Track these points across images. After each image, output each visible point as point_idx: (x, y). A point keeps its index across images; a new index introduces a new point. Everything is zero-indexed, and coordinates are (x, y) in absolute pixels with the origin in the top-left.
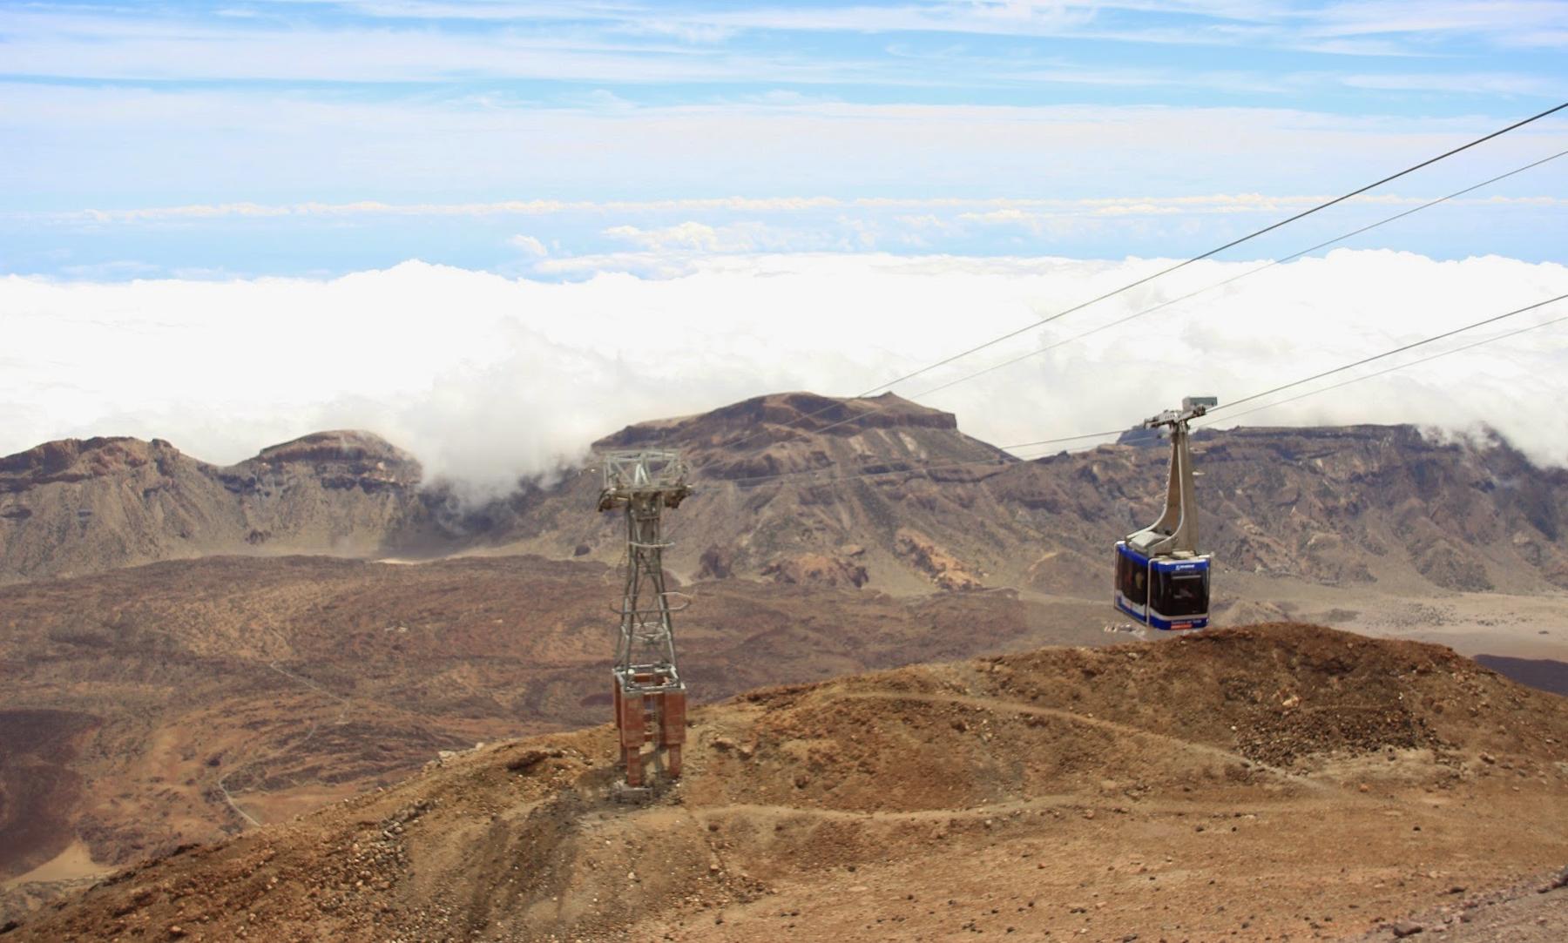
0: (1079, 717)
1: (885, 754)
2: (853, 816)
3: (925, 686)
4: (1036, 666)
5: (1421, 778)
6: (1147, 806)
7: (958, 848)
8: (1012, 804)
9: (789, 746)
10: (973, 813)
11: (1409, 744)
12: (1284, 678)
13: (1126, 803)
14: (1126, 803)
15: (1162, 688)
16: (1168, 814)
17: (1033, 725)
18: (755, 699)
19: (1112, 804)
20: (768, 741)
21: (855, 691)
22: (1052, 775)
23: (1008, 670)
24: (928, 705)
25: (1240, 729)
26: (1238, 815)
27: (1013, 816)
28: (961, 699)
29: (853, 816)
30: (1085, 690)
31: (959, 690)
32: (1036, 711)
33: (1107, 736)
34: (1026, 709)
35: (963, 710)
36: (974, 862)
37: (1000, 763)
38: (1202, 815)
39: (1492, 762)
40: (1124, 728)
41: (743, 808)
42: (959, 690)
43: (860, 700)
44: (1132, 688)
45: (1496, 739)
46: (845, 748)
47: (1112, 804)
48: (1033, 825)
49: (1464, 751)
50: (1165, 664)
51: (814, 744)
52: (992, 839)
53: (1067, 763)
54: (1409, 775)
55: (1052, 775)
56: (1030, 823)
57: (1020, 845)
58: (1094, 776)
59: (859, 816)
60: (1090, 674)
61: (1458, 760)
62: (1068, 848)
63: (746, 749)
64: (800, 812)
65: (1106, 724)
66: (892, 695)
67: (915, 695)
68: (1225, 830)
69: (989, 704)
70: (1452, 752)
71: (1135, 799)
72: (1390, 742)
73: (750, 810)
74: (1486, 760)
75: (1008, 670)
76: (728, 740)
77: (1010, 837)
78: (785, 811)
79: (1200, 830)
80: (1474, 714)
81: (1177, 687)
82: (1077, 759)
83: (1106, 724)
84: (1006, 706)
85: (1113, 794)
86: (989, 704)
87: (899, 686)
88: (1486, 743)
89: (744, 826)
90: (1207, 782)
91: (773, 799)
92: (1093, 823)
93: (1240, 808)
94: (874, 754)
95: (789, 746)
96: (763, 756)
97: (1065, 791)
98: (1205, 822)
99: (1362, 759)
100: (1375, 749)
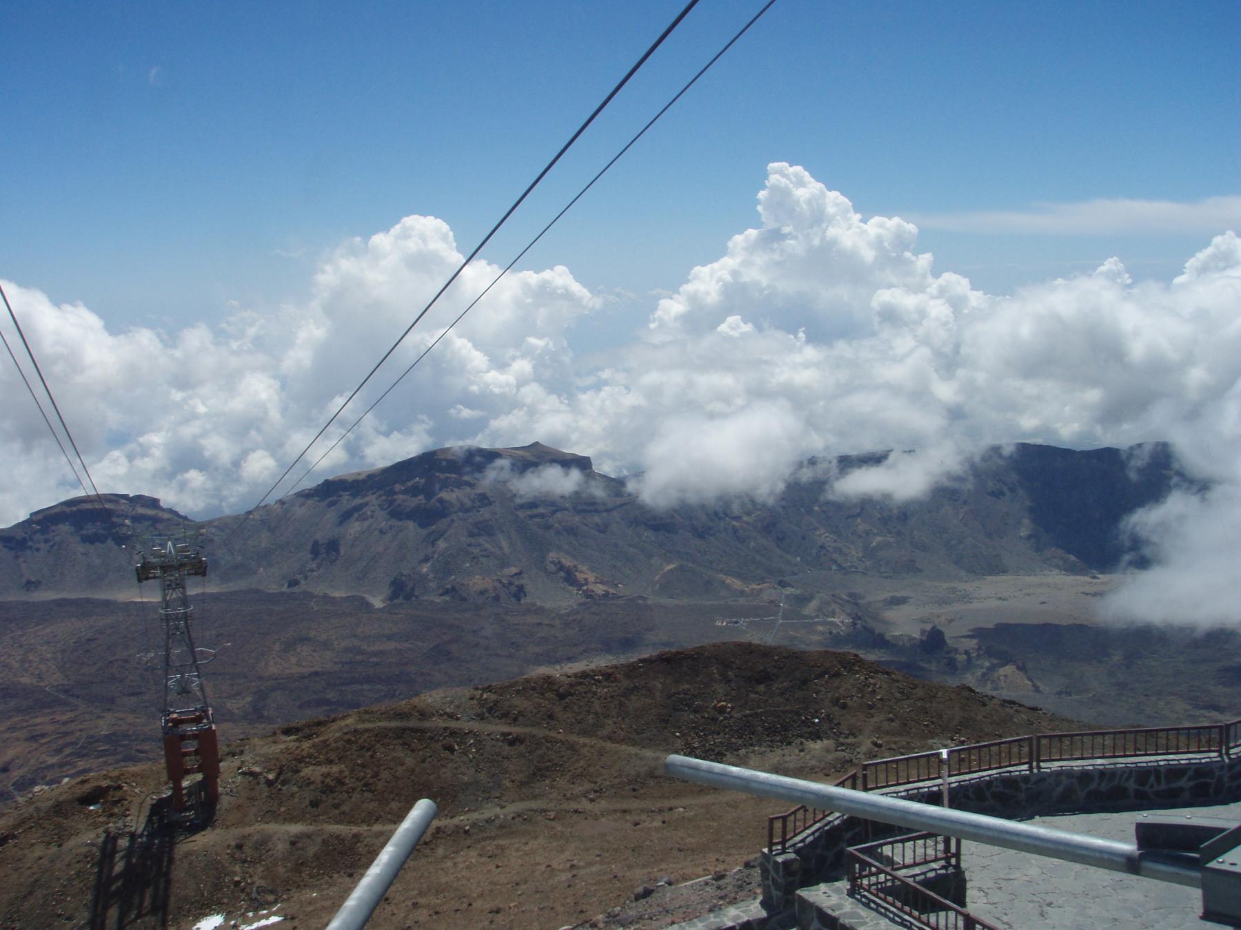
0: (553, 734)
1: (385, 775)
2: (355, 829)
3: (423, 715)
4: (518, 692)
5: (822, 765)
6: (603, 804)
7: (440, 851)
8: (490, 811)
9: (307, 771)
10: (456, 820)
11: (816, 736)
12: (720, 688)
13: (585, 805)
14: (585, 805)
15: (621, 705)
16: (615, 811)
17: (512, 743)
18: (287, 732)
19: (573, 805)
20: (287, 770)
21: (364, 721)
22: (522, 784)
23: (493, 697)
24: (423, 731)
25: (683, 735)
26: (671, 809)
27: (489, 821)
28: (453, 724)
29: (355, 829)
30: (557, 709)
31: (452, 716)
32: (516, 730)
33: (572, 748)
34: (506, 729)
35: (453, 733)
36: (449, 863)
37: (483, 777)
38: (643, 811)
39: (880, 746)
40: (587, 740)
41: (265, 826)
42: (452, 716)
43: (367, 730)
44: (597, 706)
45: (886, 725)
46: (352, 771)
47: (573, 805)
48: (506, 829)
49: (860, 738)
50: (626, 683)
51: (324, 769)
52: (469, 842)
53: (541, 772)
54: (813, 762)
55: (522, 784)
56: (502, 827)
57: (490, 847)
58: (561, 782)
59: (363, 829)
60: (562, 697)
61: (852, 746)
62: (527, 848)
63: (271, 777)
64: (311, 828)
65: (574, 738)
66: (394, 724)
67: (413, 723)
68: (657, 824)
69: (476, 726)
70: (851, 740)
71: (592, 800)
72: (801, 736)
73: (272, 827)
74: (875, 744)
75: (493, 697)
76: (257, 769)
77: (484, 839)
78: (296, 828)
79: (636, 824)
80: (871, 707)
81: (635, 702)
82: (547, 769)
83: (574, 738)
84: (490, 728)
85: (574, 798)
86: (476, 726)
87: (400, 715)
88: (878, 729)
89: (263, 843)
90: (651, 782)
91: (292, 819)
92: (554, 824)
93: (674, 803)
94: (376, 775)
95: (307, 771)
96: (284, 783)
97: (535, 797)
98: (644, 817)
99: (779, 752)
100: (790, 744)
